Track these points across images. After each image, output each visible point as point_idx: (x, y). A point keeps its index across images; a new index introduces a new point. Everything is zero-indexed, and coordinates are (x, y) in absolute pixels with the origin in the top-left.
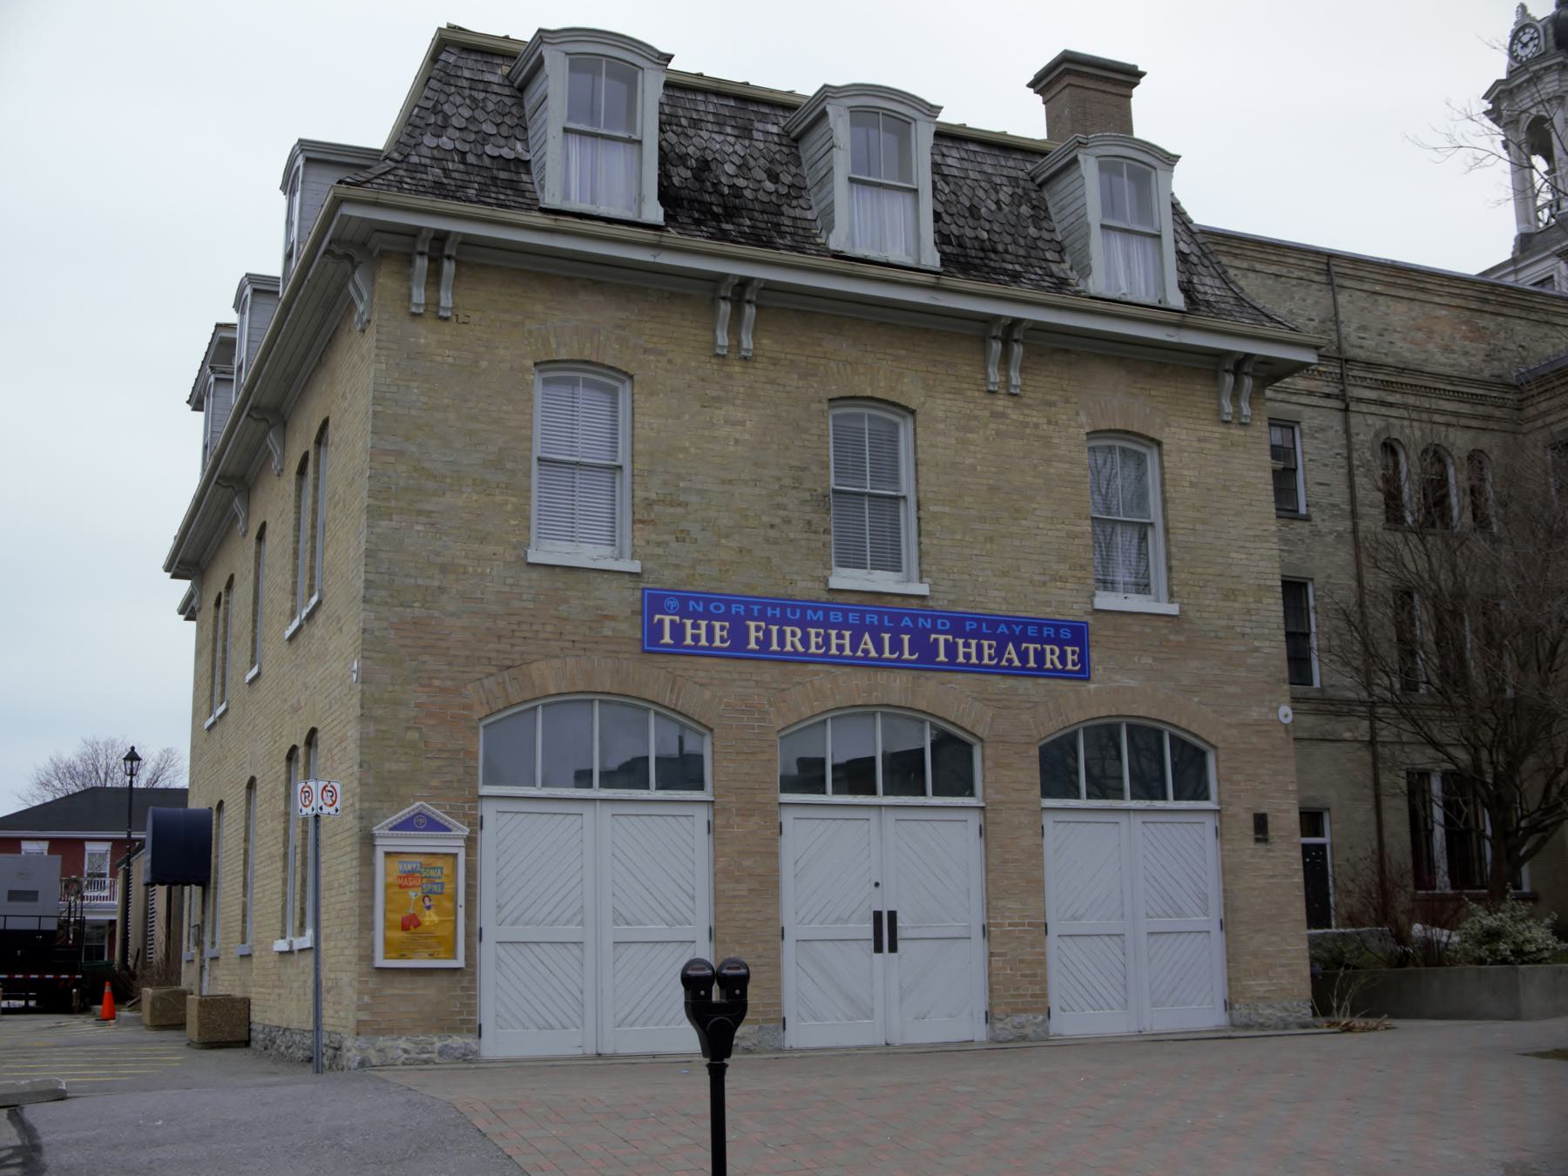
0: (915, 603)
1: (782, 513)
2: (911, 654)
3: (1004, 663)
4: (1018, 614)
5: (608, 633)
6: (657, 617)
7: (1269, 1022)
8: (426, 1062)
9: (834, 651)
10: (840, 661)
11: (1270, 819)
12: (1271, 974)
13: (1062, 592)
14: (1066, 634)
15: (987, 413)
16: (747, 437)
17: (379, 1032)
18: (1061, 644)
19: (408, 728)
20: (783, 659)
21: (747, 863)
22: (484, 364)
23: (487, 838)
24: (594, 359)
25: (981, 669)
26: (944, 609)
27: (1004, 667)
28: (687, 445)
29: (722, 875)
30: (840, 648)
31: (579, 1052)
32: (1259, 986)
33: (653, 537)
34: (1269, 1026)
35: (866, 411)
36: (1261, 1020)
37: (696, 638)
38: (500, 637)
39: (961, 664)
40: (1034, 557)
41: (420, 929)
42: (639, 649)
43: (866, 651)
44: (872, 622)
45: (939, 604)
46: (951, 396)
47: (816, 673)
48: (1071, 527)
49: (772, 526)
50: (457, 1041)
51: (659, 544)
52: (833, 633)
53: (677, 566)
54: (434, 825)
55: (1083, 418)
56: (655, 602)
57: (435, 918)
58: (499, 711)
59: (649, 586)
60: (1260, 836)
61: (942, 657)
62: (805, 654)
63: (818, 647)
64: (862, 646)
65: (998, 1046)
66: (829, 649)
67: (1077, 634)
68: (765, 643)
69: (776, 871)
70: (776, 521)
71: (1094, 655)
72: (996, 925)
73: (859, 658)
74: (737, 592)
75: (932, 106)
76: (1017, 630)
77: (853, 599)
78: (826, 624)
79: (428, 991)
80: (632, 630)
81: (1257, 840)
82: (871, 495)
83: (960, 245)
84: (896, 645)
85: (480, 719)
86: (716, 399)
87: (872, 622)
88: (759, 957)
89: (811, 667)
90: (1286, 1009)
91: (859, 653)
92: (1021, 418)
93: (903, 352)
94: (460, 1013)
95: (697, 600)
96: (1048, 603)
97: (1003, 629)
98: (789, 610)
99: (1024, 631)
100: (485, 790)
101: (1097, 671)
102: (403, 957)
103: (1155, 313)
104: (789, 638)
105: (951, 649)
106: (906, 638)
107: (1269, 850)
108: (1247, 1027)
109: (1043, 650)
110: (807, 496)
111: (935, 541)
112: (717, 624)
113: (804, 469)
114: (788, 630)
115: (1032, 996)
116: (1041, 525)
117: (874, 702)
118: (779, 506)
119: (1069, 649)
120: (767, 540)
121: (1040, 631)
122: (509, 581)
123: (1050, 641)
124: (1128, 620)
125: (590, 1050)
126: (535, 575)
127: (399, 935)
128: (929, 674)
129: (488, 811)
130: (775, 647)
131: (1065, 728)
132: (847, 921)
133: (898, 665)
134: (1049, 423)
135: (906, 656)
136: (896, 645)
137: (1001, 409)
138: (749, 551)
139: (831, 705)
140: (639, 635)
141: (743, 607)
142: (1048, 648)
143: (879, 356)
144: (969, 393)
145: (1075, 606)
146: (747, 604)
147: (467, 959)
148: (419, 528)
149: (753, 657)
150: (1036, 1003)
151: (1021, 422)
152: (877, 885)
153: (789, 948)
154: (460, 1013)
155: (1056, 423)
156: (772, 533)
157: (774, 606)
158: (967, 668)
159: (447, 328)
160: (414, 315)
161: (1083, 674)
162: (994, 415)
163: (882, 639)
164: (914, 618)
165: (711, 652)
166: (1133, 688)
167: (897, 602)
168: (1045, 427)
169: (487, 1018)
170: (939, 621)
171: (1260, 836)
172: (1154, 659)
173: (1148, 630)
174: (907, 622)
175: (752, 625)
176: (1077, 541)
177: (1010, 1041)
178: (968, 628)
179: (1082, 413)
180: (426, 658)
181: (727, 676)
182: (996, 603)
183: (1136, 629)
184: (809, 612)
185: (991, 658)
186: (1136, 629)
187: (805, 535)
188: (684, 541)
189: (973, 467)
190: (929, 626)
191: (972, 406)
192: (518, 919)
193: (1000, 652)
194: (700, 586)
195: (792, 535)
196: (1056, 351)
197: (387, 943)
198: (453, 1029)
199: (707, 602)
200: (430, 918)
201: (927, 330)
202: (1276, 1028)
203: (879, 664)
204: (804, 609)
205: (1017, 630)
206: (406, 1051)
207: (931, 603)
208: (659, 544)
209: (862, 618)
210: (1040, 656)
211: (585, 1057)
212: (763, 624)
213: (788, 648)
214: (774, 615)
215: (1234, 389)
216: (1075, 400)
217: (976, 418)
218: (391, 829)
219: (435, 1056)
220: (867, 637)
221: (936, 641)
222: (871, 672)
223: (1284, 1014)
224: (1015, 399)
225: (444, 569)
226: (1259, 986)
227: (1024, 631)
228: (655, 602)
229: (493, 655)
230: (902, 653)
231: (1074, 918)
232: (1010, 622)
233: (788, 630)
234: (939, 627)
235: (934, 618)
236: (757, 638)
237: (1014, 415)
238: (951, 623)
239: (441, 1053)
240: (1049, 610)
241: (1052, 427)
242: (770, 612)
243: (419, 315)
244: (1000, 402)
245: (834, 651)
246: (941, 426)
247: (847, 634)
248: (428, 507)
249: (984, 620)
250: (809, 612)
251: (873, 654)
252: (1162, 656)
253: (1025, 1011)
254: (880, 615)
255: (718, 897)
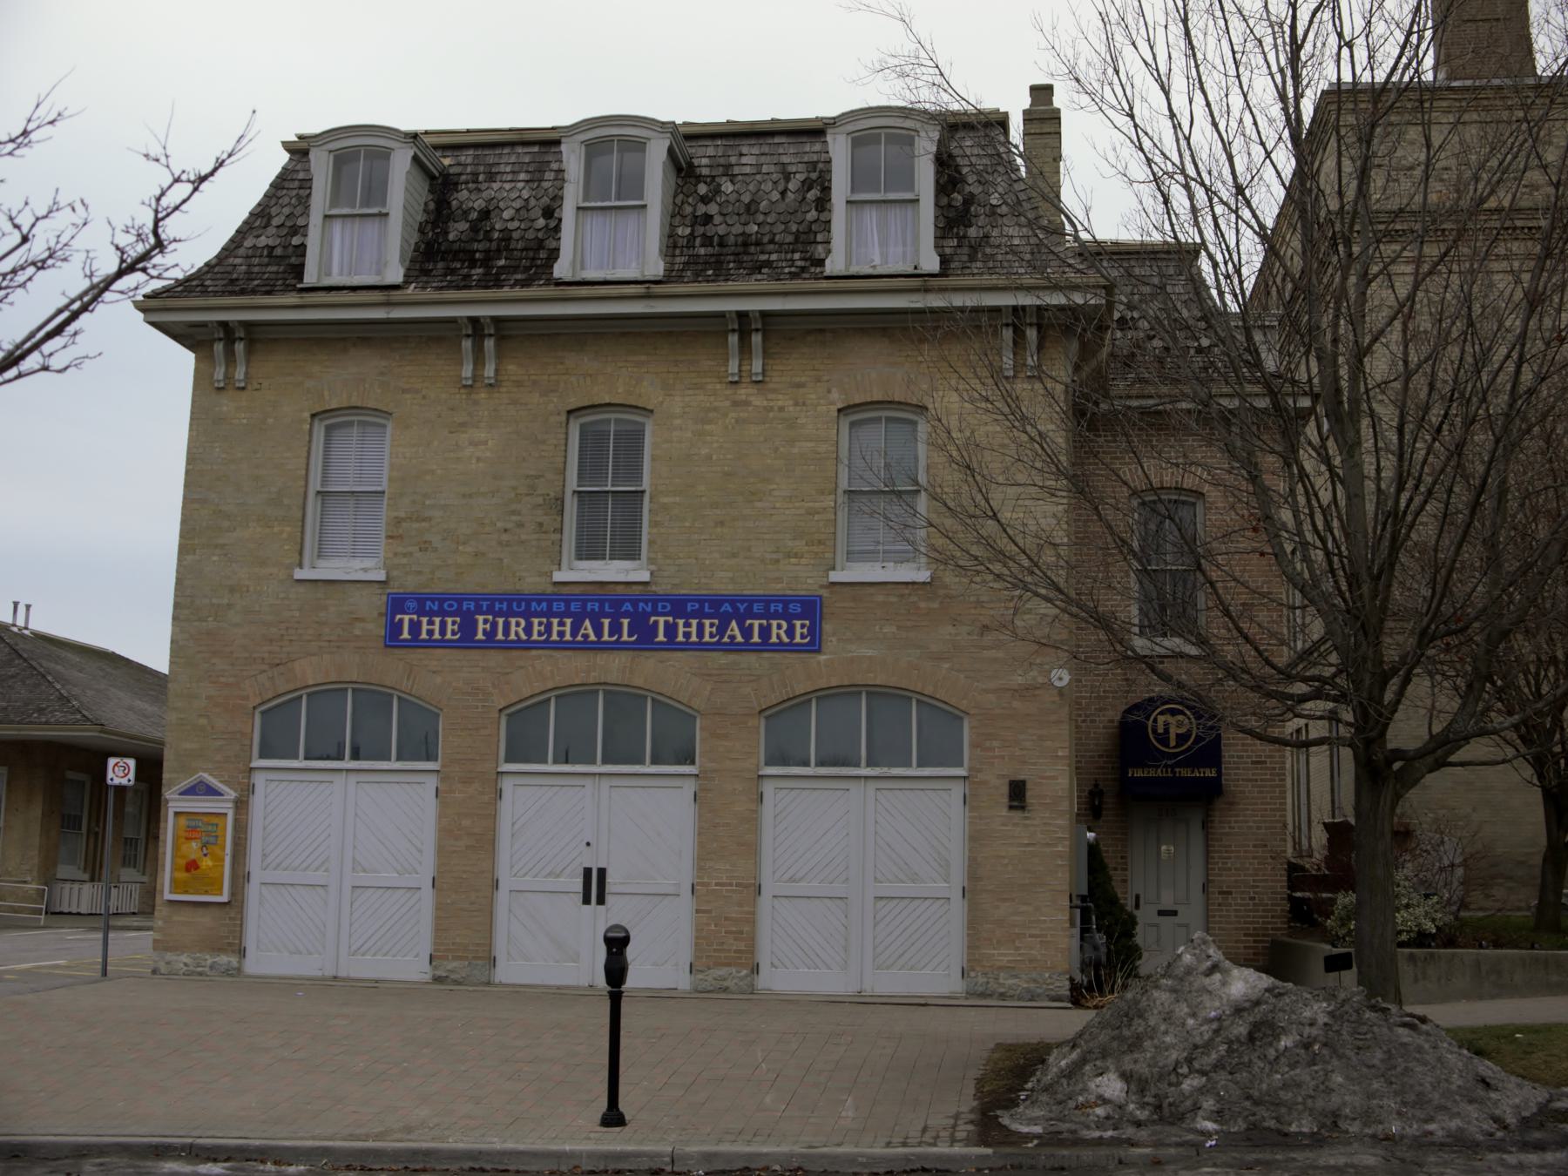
0: (637, 590)
1: (514, 518)
2: (630, 635)
3: (726, 639)
4: (745, 592)
5: (357, 632)
6: (398, 617)
7: (1011, 992)
8: (200, 974)
9: (555, 637)
10: (561, 646)
11: (1029, 786)
12: (1017, 944)
13: (798, 568)
14: (795, 608)
15: (727, 403)
16: (488, 454)
17: (167, 949)
18: (789, 618)
19: (201, 716)
20: (507, 646)
21: (466, 823)
22: (270, 421)
23: (258, 802)
24: (359, 404)
25: (701, 646)
26: (668, 592)
27: (726, 644)
28: (435, 467)
29: (447, 832)
30: (562, 634)
31: (320, 974)
32: (1003, 955)
33: (400, 549)
34: (1011, 996)
35: (613, 416)
36: (1002, 990)
37: (430, 632)
38: (271, 641)
39: (681, 643)
40: (767, 536)
41: (198, 871)
42: (382, 644)
43: (586, 636)
44: (593, 610)
45: (660, 589)
46: (691, 392)
47: (539, 657)
48: (811, 504)
49: (506, 530)
50: (223, 959)
51: (405, 555)
52: (555, 621)
53: (420, 573)
54: (211, 791)
55: (835, 395)
56: (397, 604)
57: (210, 863)
58: (269, 700)
59: (395, 591)
60: (1016, 804)
61: (661, 637)
62: (527, 641)
63: (540, 634)
64: (582, 631)
65: (700, 993)
66: (550, 634)
67: (810, 608)
68: (491, 634)
69: (493, 829)
70: (509, 526)
71: (827, 627)
72: (703, 884)
73: (579, 642)
74: (468, 591)
75: (663, 123)
76: (742, 608)
77: (577, 590)
78: (549, 614)
79: (205, 919)
80: (378, 629)
81: (1011, 808)
82: (613, 492)
83: (721, 245)
84: (616, 629)
85: (254, 708)
86: (463, 425)
87: (593, 610)
88: (472, 903)
89: (534, 652)
90: (1035, 981)
91: (579, 638)
92: (765, 403)
93: (643, 358)
94: (227, 937)
95: (433, 600)
96: (779, 580)
97: (727, 607)
98: (515, 604)
99: (750, 608)
100: (257, 763)
101: (831, 642)
102: (186, 892)
103: (919, 280)
104: (513, 628)
105: (671, 630)
106: (626, 622)
107: (1026, 818)
108: (983, 995)
109: (769, 626)
110: (540, 500)
111: (662, 530)
112: (449, 620)
113: (537, 477)
114: (513, 621)
115: (735, 951)
116: (778, 505)
117: (592, 681)
118: (513, 513)
119: (798, 623)
120: (500, 543)
121: (767, 608)
122: (282, 595)
123: (776, 616)
124: (872, 590)
125: (330, 972)
126: (301, 589)
127: (182, 875)
128: (647, 654)
129: (259, 780)
130: (500, 636)
131: (789, 699)
132: (558, 876)
133: (618, 646)
134: (796, 404)
135: (625, 637)
136: (616, 629)
137: (744, 397)
138: (483, 554)
139: (550, 685)
140: (383, 633)
141: (473, 604)
142: (774, 623)
143: (620, 364)
144: (710, 387)
145: (809, 581)
146: (477, 601)
147: (233, 894)
148: (215, 558)
149: (480, 646)
150: (740, 958)
151: (765, 407)
152: (588, 844)
153: (502, 896)
154: (227, 937)
155: (804, 404)
156: (505, 537)
157: (501, 601)
158: (687, 646)
159: (244, 394)
160: (219, 389)
161: (814, 644)
162: (736, 404)
163: (602, 624)
164: (635, 603)
165: (443, 644)
166: (870, 657)
167: (620, 590)
168: (791, 409)
169: (250, 943)
170: (660, 605)
171: (1016, 804)
172: (899, 628)
173: (893, 599)
174: (628, 607)
175: (481, 618)
176: (817, 517)
177: (709, 992)
178: (689, 609)
179: (834, 390)
180: (214, 661)
181: (457, 664)
182: (722, 583)
183: (880, 598)
184: (534, 604)
185: (712, 636)
186: (880, 598)
187: (535, 536)
188: (426, 550)
189: (709, 457)
190: (649, 609)
191: (712, 398)
192: (278, 865)
193: (722, 630)
194: (438, 588)
195: (523, 537)
196: (809, 332)
197: (173, 881)
198: (220, 950)
199: (442, 601)
200: (206, 863)
201: (670, 333)
202: (1019, 999)
203: (600, 646)
204: (528, 602)
205: (742, 608)
206: (186, 965)
207: (654, 588)
208: (405, 555)
209: (584, 607)
210: (765, 632)
211: (323, 979)
212: (490, 617)
213: (513, 637)
214: (501, 609)
215: (1015, 343)
216: (825, 378)
217: (715, 409)
218: (181, 794)
219: (207, 969)
220: (587, 623)
221: (656, 623)
222: (591, 654)
223: (1032, 986)
224: (760, 386)
225: (232, 590)
226: (1003, 955)
227: (750, 608)
228: (397, 604)
229: (266, 655)
230: (620, 636)
231: (792, 880)
232: (733, 601)
233: (513, 621)
234: (660, 610)
235: (655, 603)
236: (484, 630)
237: (758, 401)
238: (672, 605)
239: (211, 967)
240: (779, 586)
241: (798, 408)
242: (497, 606)
243: (222, 388)
244: (743, 391)
245: (555, 637)
246: (678, 422)
247: (568, 621)
248: (221, 541)
249: (705, 601)
250: (534, 604)
251: (593, 638)
252: (909, 624)
253: (729, 965)
254: (602, 603)
255: (441, 851)
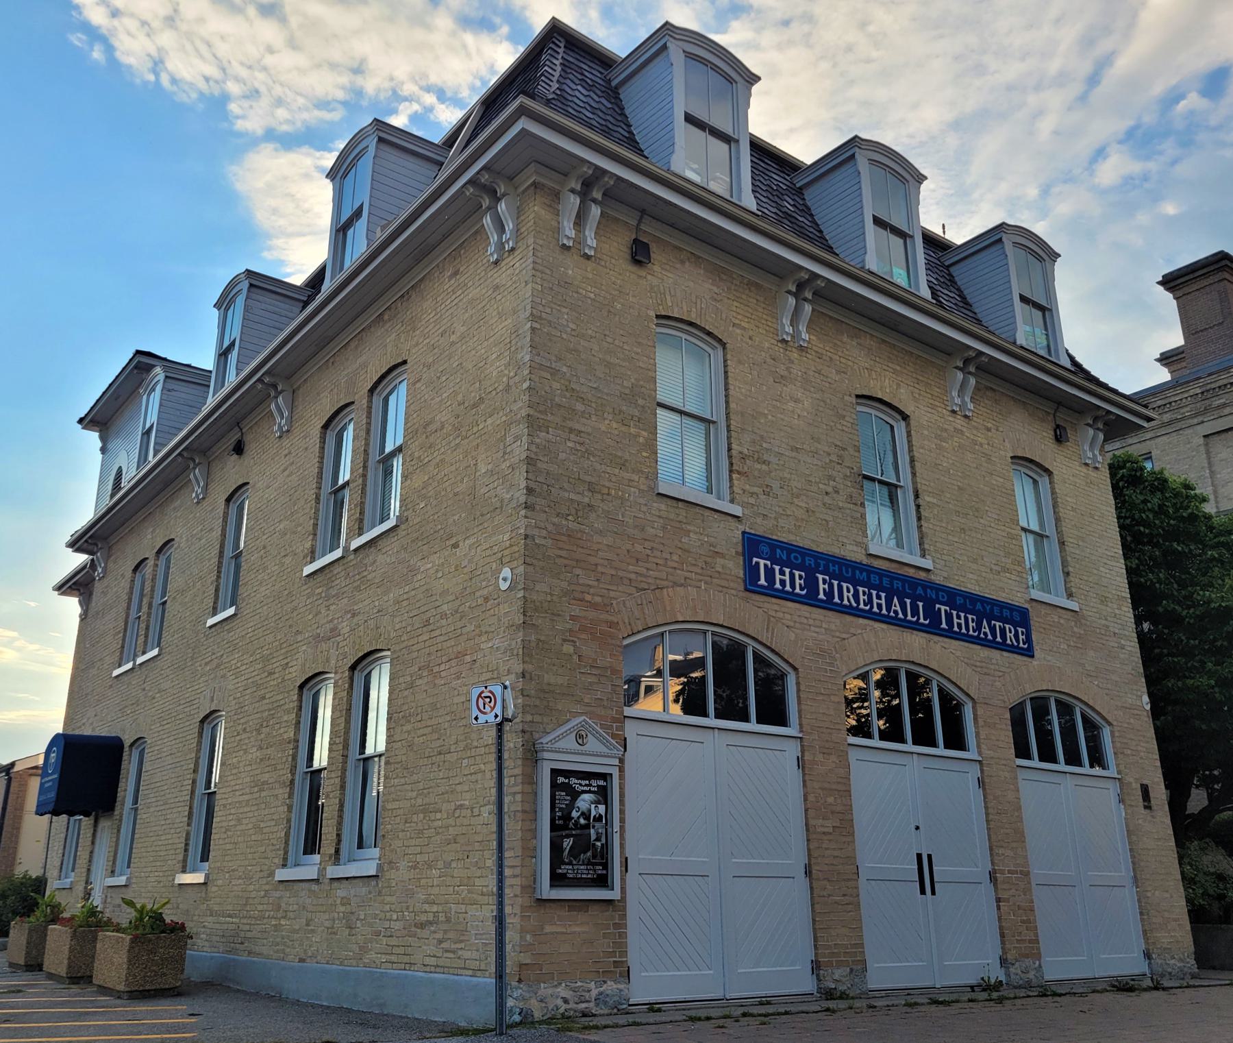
2: (925, 619)
21: (830, 800)
42: (742, 588)
43: (896, 612)
45: (937, 579)
70: (830, 490)
89: (861, 621)
95: (782, 549)
96: (1002, 589)
104: (845, 594)
113: (844, 449)
114: (845, 585)
116: (992, 525)
118: (831, 478)
126: (662, 505)
130: (836, 600)
133: (915, 627)
134: (988, 444)
135: (922, 620)
136: (915, 612)
140: (741, 575)
152: (917, 828)
159: (590, 265)
163: (905, 603)
165: (791, 597)
175: (820, 577)
178: (958, 602)
180: (578, 571)
195: (841, 504)
206: (566, 1001)
208: (752, 494)
213: (846, 602)
230: (919, 619)
236: (824, 589)
243: (568, 248)
248: (577, 426)
